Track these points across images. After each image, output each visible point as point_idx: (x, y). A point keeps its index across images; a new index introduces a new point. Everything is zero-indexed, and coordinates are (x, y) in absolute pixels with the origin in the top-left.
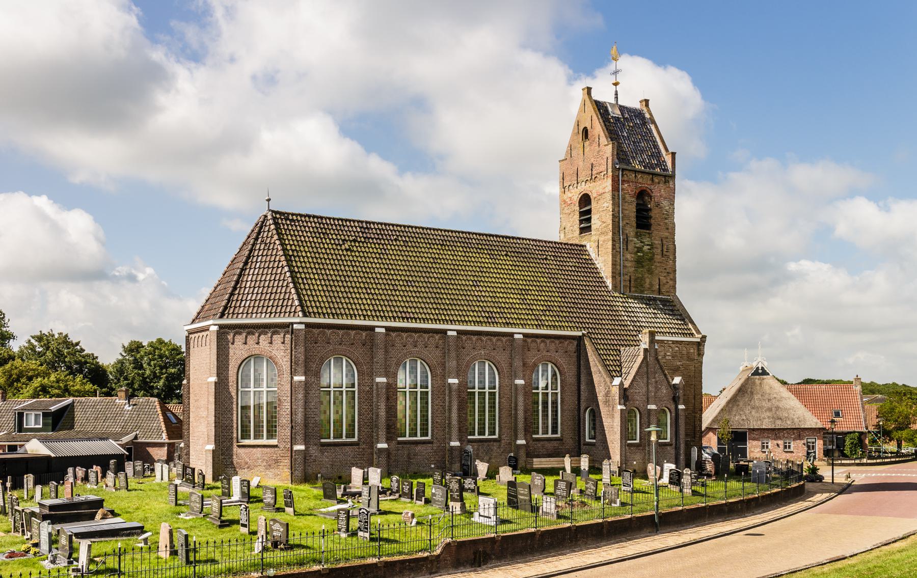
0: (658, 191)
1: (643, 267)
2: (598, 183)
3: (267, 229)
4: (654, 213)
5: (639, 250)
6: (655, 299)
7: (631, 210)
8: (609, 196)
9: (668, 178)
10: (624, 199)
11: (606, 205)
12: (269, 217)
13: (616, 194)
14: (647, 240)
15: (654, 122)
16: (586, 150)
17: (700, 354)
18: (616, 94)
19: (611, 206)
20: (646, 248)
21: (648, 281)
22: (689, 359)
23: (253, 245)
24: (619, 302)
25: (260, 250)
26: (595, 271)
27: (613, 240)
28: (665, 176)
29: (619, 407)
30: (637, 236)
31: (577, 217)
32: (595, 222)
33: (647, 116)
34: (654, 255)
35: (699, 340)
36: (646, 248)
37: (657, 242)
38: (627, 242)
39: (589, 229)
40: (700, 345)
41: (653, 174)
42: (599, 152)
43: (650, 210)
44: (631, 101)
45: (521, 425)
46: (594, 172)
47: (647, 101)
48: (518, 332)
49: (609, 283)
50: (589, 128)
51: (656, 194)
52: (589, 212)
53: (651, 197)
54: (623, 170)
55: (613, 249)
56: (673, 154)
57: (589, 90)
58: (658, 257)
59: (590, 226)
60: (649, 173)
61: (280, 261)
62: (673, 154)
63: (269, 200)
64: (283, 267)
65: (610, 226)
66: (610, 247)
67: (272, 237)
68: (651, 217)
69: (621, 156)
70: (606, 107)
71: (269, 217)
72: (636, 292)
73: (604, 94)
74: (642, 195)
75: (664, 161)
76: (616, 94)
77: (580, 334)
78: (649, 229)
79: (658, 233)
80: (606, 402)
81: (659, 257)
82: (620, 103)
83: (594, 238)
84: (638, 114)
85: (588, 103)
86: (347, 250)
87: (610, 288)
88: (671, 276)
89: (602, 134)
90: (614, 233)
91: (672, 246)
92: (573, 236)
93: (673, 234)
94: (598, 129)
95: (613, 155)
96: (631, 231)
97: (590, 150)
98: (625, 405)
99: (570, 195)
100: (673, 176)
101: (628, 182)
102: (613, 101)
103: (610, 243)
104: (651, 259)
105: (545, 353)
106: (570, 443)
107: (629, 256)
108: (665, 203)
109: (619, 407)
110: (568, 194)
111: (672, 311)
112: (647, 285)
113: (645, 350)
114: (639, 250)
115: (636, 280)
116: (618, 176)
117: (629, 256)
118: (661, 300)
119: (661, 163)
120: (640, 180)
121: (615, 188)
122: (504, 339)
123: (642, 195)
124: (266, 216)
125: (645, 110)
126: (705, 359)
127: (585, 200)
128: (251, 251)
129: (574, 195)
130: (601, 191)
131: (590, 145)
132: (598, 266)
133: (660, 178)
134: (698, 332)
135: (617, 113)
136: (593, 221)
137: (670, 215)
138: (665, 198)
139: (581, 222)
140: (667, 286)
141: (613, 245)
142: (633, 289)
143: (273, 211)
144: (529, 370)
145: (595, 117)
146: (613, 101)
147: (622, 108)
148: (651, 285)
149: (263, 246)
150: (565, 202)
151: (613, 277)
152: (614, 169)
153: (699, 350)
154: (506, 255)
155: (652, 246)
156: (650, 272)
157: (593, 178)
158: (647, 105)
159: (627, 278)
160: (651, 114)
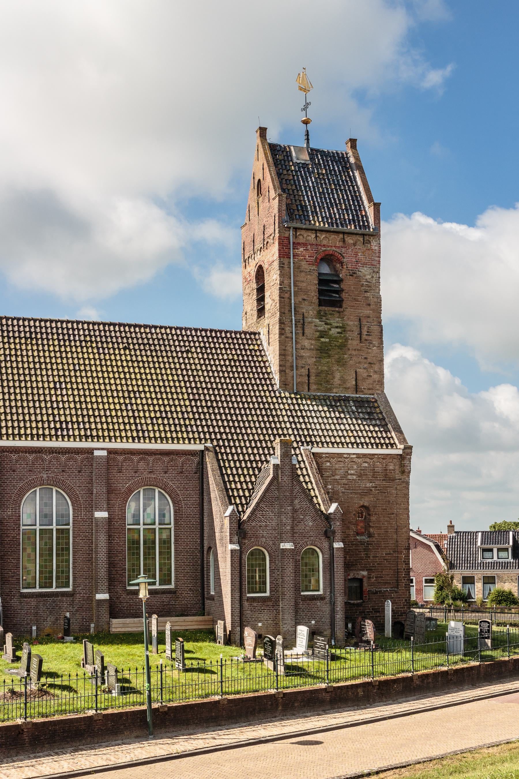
1: (329, 357)
5: (323, 334)
6: (347, 399)
13: (286, 261)
14: (335, 321)
15: (360, 168)
17: (405, 471)
21: (338, 375)
22: (388, 477)
24: (285, 405)
28: (363, 235)
29: (231, 547)
30: (320, 315)
33: (352, 160)
34: (347, 340)
35: (400, 452)
37: (352, 323)
38: (302, 324)
40: (404, 459)
41: (344, 233)
43: (342, 280)
45: (102, 572)
46: (266, 236)
48: (100, 448)
49: (276, 378)
51: (348, 258)
53: (342, 263)
54: (296, 229)
55: (281, 334)
58: (353, 343)
68: (342, 290)
70: (290, 151)
72: (318, 390)
77: (201, 447)
78: (341, 307)
80: (221, 539)
82: (312, 146)
84: (341, 159)
87: (277, 387)
88: (376, 368)
90: (282, 313)
91: (375, 328)
95: (279, 211)
96: (310, 310)
98: (240, 543)
100: (376, 234)
101: (305, 245)
104: (343, 346)
105: (146, 475)
106: (188, 597)
107: (306, 343)
108: (365, 271)
109: (231, 547)
111: (368, 413)
112: (337, 381)
113: (276, 466)
115: (318, 375)
116: (288, 238)
117: (306, 343)
118: (355, 401)
119: (359, 219)
120: (325, 242)
122: (79, 457)
125: (350, 154)
126: (413, 478)
127: (260, 273)
130: (271, 259)
133: (356, 238)
134: (403, 440)
135: (305, 157)
137: (373, 286)
138: (365, 264)
140: (370, 381)
142: (313, 387)
144: (116, 498)
145: (266, 166)
147: (313, 153)
148: (343, 381)
151: (281, 371)
153: (402, 466)
155: (344, 328)
156: (341, 362)
157: (266, 245)
159: (304, 371)
160: (357, 158)
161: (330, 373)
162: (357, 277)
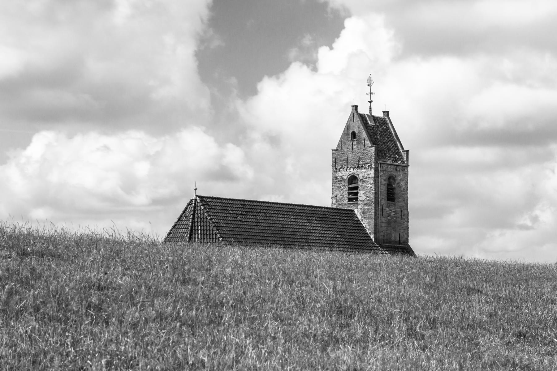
0: (399, 176)
1: (391, 226)
2: (364, 170)
3: (199, 208)
4: (397, 191)
5: (389, 215)
7: (383, 189)
8: (372, 181)
9: (405, 167)
10: (381, 182)
11: (369, 186)
12: (199, 201)
13: (377, 179)
16: (355, 147)
18: (370, 108)
19: (373, 187)
20: (393, 213)
21: (393, 235)
23: (193, 218)
25: (198, 222)
26: (363, 229)
27: (375, 210)
30: (388, 206)
31: (346, 190)
32: (362, 195)
36: (393, 213)
37: (399, 210)
39: (357, 199)
41: (396, 165)
42: (364, 150)
44: (378, 113)
46: (361, 163)
47: (388, 112)
49: (372, 237)
50: (357, 132)
52: (357, 188)
56: (407, 151)
57: (356, 107)
59: (357, 198)
60: (394, 165)
61: (213, 230)
62: (407, 151)
63: (196, 189)
64: (216, 234)
65: (373, 200)
66: (373, 214)
67: (204, 214)
69: (380, 154)
71: (199, 201)
73: (364, 110)
74: (391, 179)
75: (402, 156)
76: (370, 108)
79: (399, 203)
81: (399, 219)
82: (372, 114)
83: (360, 206)
85: (356, 115)
86: (241, 221)
87: (373, 240)
88: (406, 231)
89: (367, 139)
91: (406, 212)
92: (344, 203)
93: (407, 204)
94: (364, 134)
96: (384, 202)
97: (357, 147)
99: (341, 175)
100: (407, 166)
102: (368, 113)
103: (373, 212)
108: (403, 184)
110: (339, 174)
114: (389, 215)
116: (378, 167)
117: (383, 219)
120: (390, 169)
121: (376, 176)
123: (391, 179)
124: (196, 200)
125: (387, 119)
127: (353, 179)
128: (192, 222)
129: (345, 174)
130: (366, 176)
131: (357, 144)
132: (364, 225)
136: (359, 195)
139: (349, 194)
141: (375, 213)
143: (199, 197)
145: (361, 127)
146: (368, 113)
147: (375, 119)
149: (199, 220)
150: (336, 178)
151: (375, 234)
152: (376, 163)
154: (316, 220)
156: (395, 229)
158: (388, 115)
159: (382, 233)
161: (391, 234)
162: (401, 187)
